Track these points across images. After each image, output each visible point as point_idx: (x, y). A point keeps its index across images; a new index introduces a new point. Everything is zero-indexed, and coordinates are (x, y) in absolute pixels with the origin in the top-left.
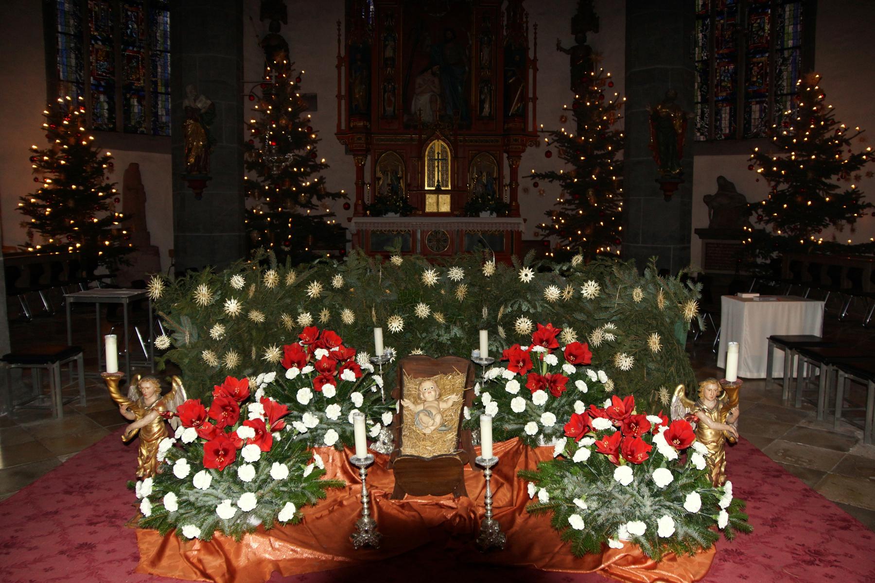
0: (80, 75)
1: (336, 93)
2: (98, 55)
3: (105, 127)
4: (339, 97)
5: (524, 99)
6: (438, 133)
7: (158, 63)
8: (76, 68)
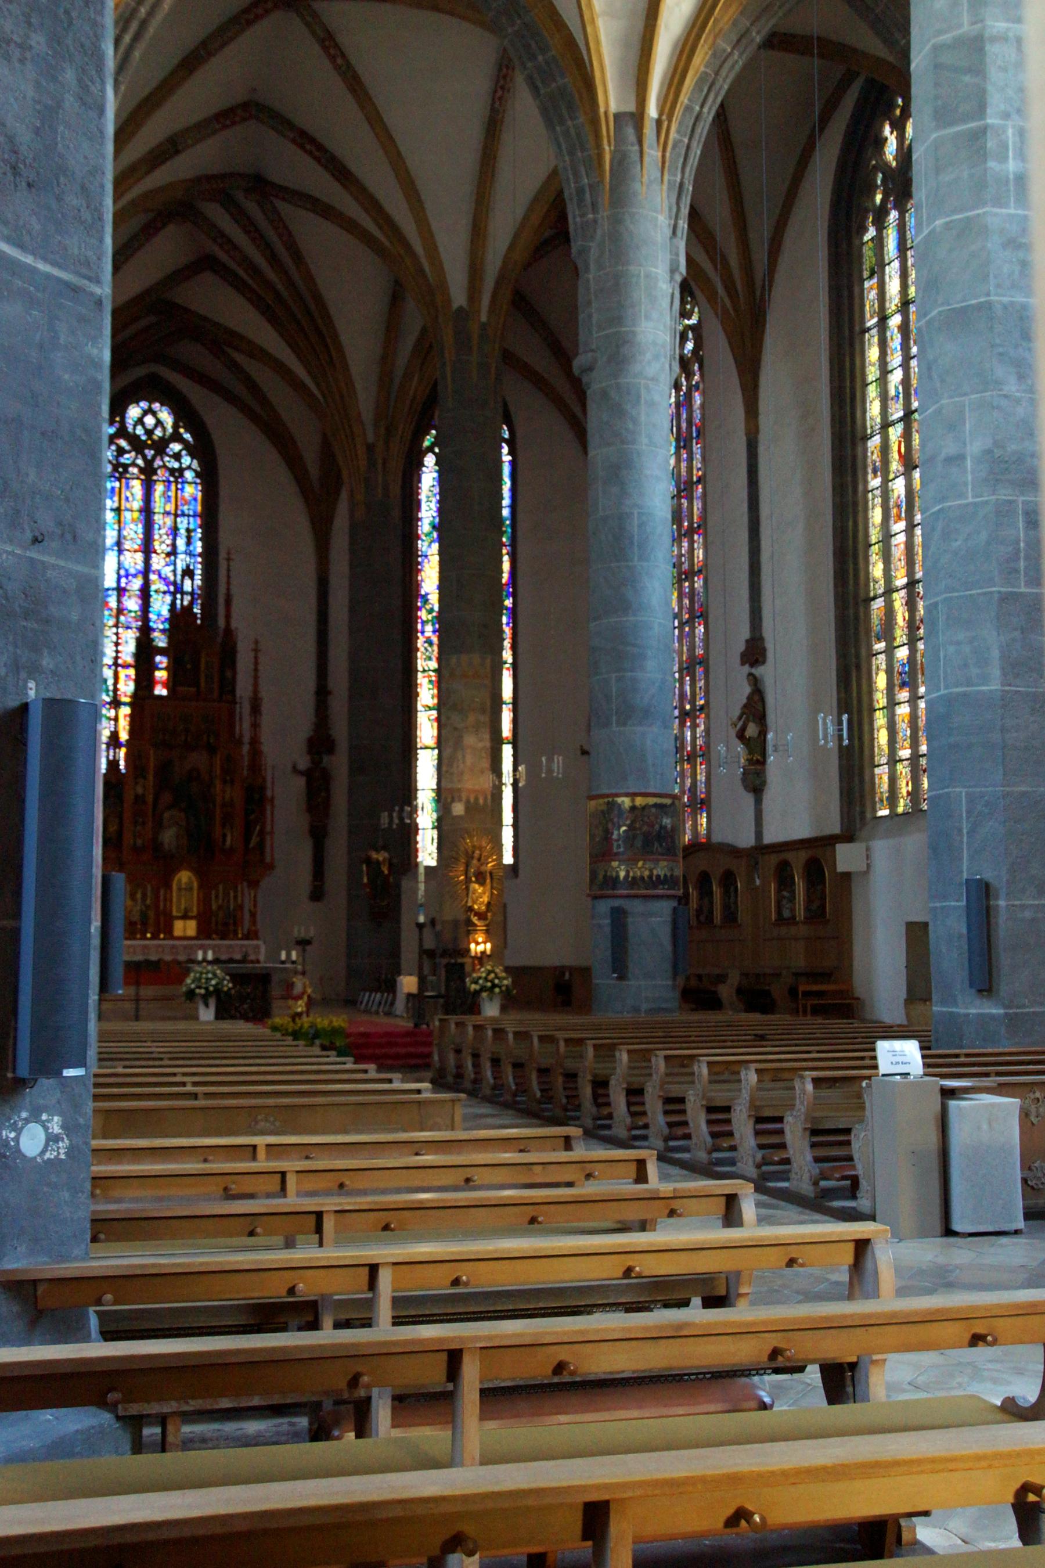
5: (262, 833)
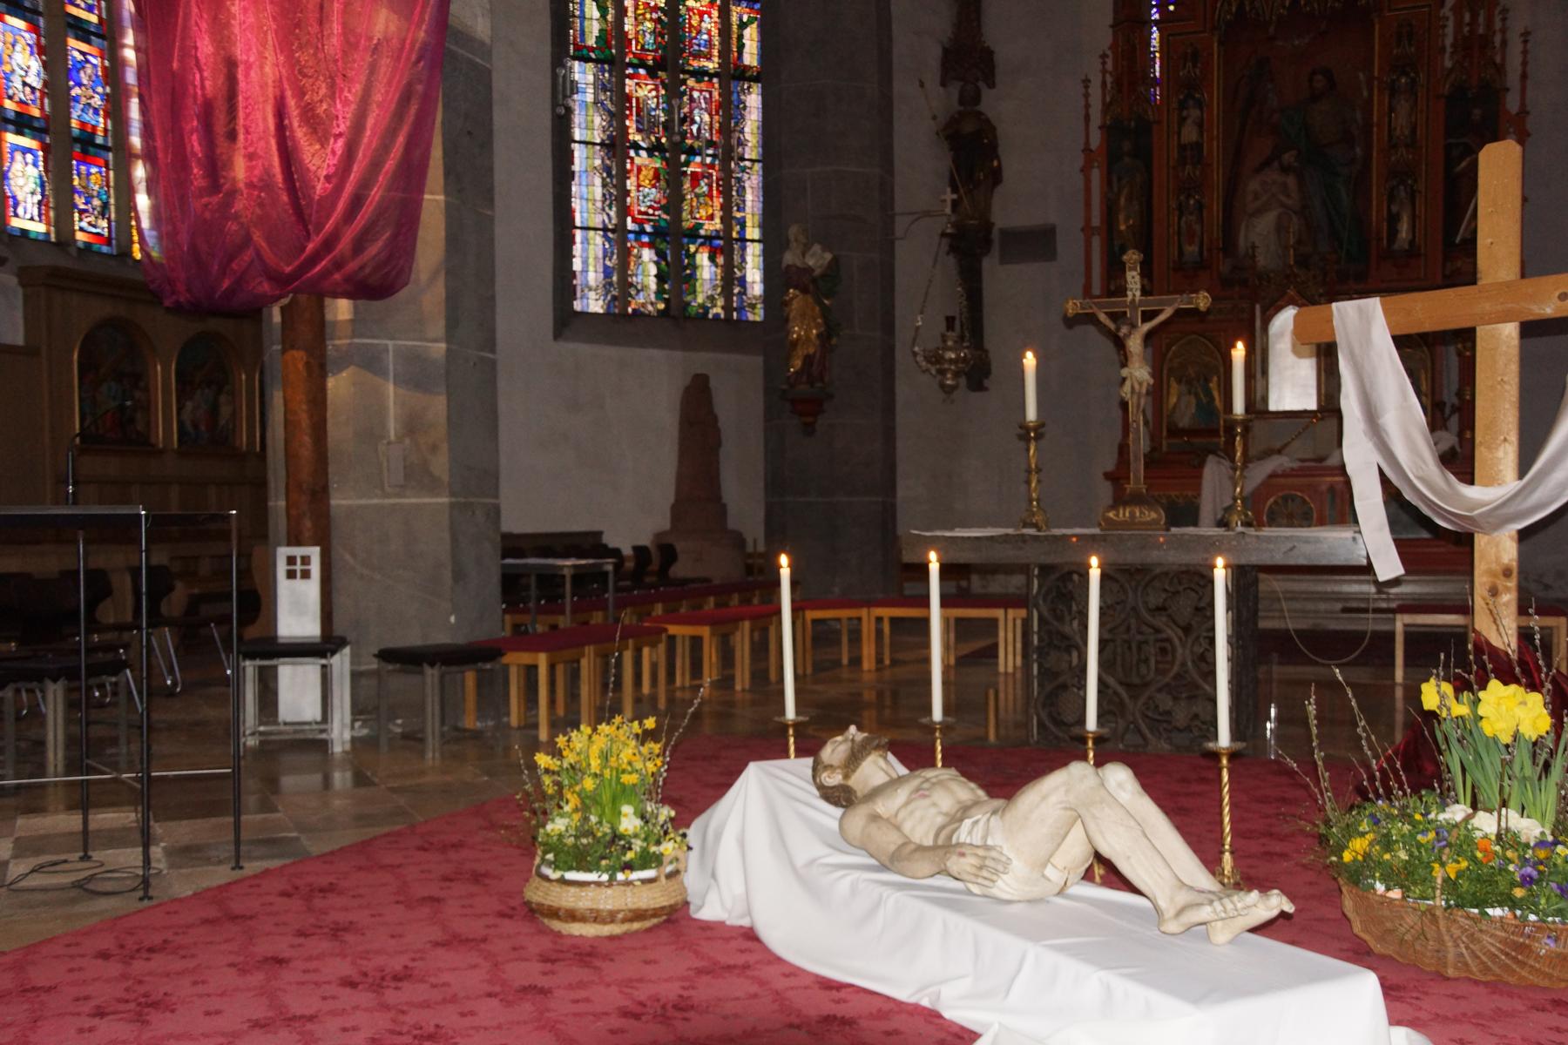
0: (608, 215)
1: (1081, 224)
2: (641, 177)
3: (650, 308)
4: (1087, 230)
6: (1291, 292)
7: (747, 184)
8: (603, 202)
